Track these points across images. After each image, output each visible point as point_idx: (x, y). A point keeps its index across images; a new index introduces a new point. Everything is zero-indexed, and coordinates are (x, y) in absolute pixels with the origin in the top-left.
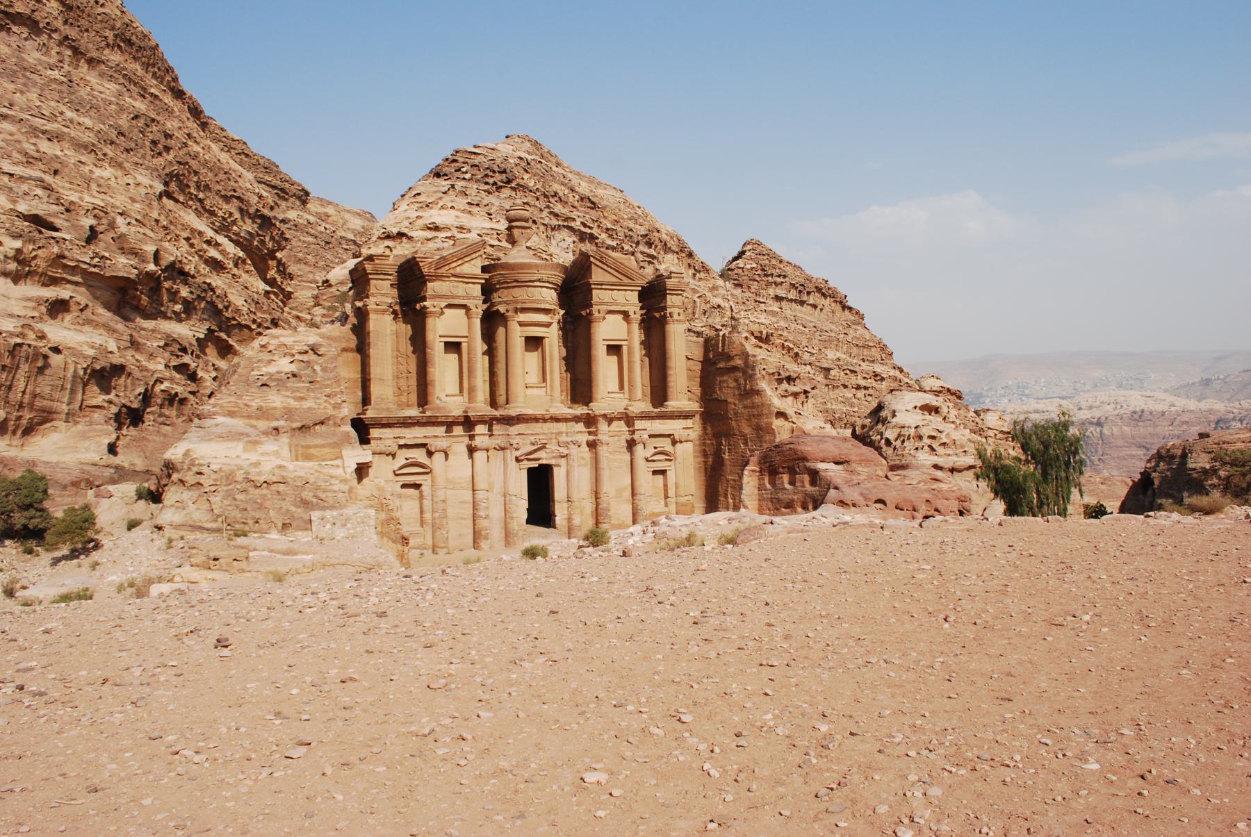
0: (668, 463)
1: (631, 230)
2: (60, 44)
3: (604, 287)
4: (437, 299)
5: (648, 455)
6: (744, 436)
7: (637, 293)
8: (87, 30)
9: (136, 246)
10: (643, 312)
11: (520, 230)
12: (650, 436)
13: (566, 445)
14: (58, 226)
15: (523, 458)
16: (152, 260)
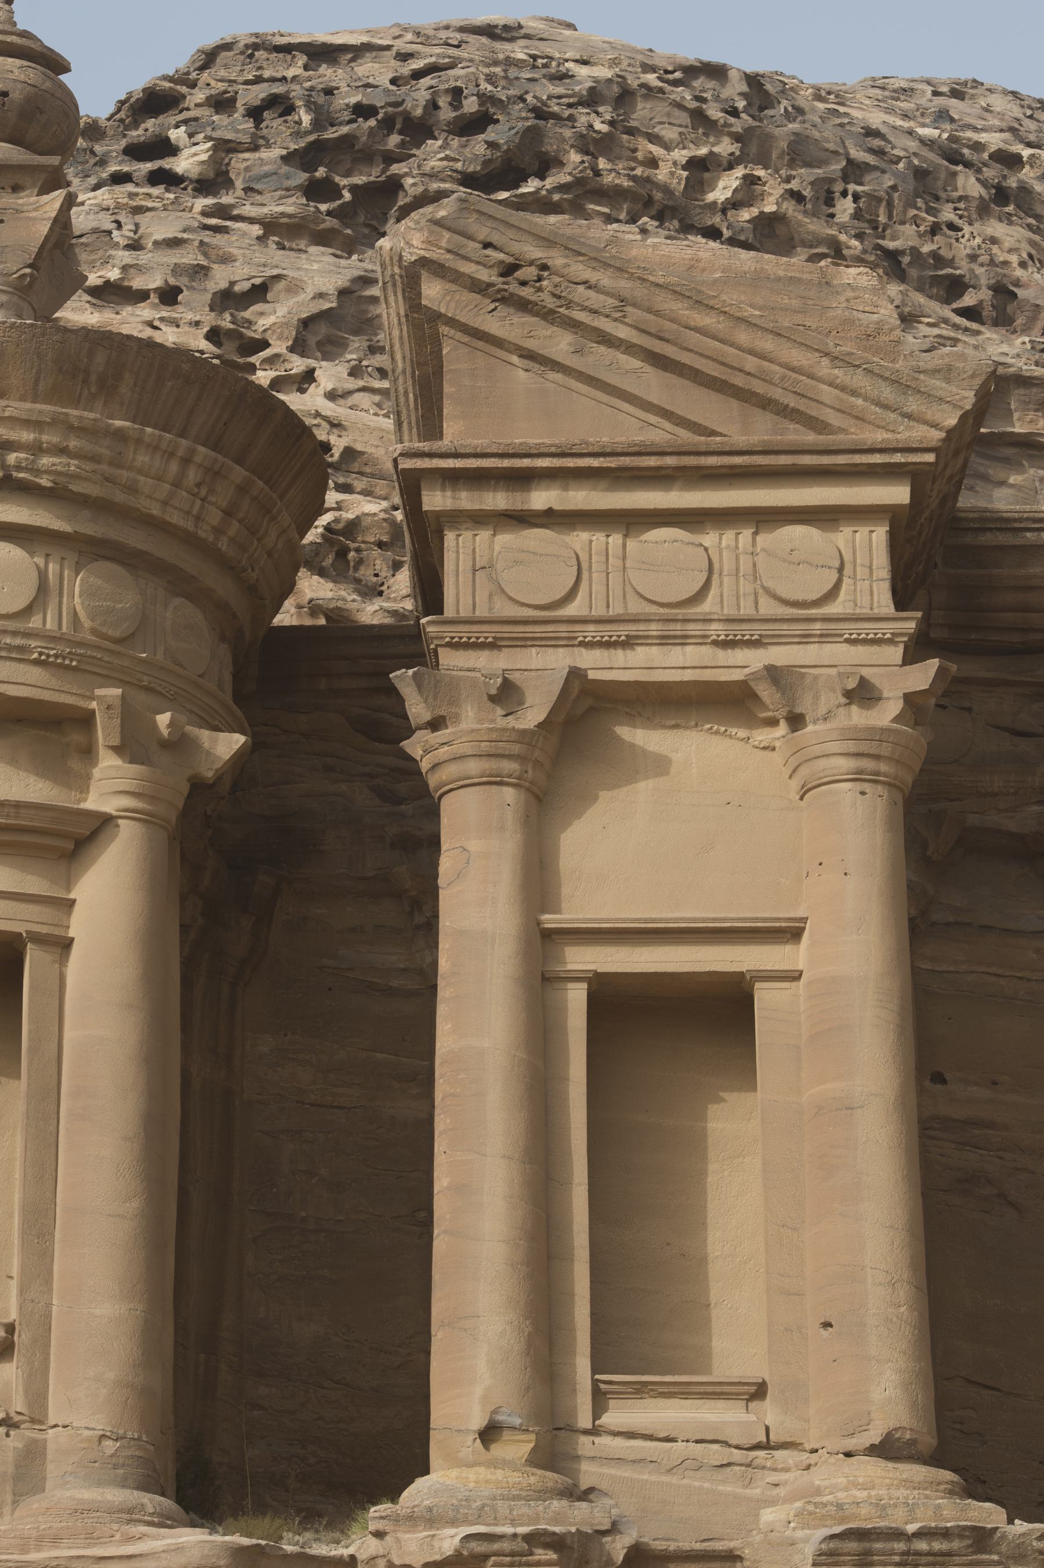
3: (541, 499)
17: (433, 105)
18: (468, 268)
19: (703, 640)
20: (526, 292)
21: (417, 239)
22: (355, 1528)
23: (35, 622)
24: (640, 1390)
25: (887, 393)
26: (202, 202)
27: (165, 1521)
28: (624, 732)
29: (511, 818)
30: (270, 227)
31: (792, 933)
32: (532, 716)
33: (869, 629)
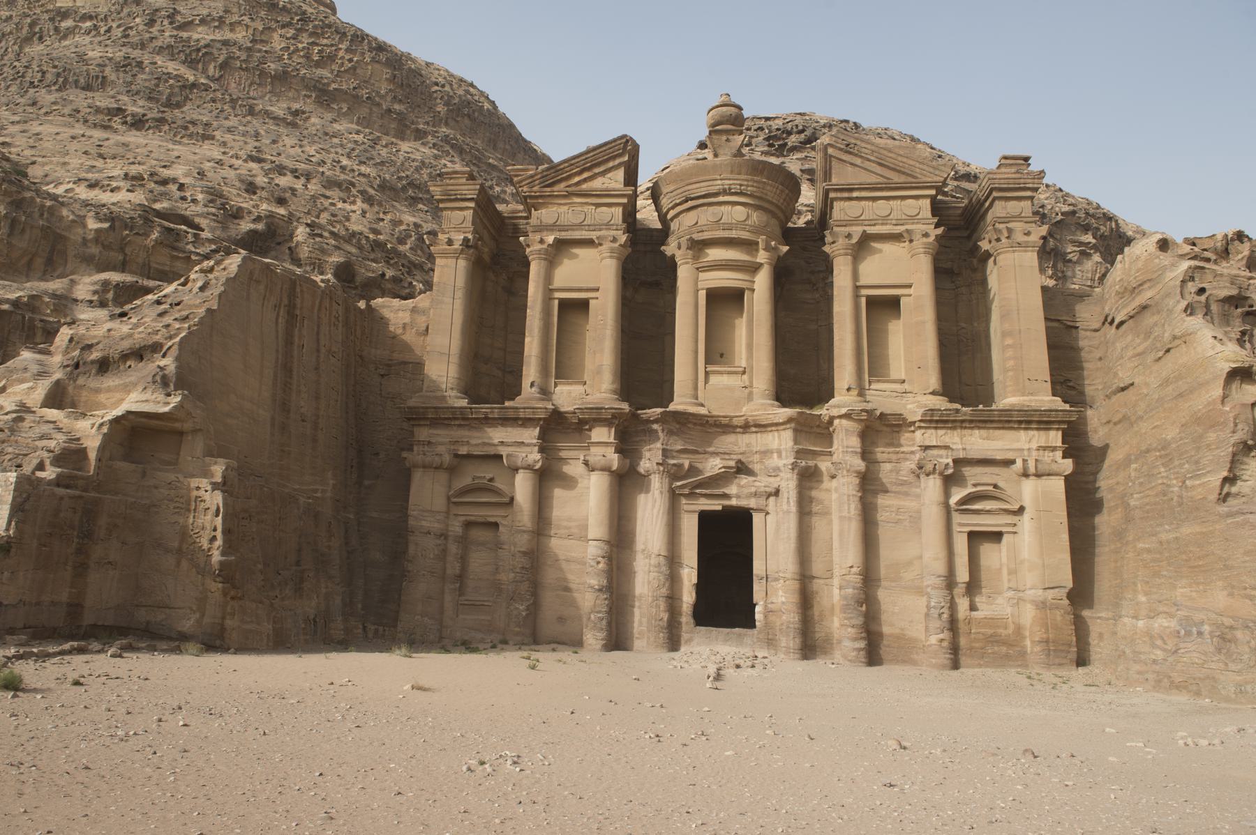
0: (1010, 519)
1: (1043, 207)
2: (382, 116)
3: (855, 194)
4: (545, 233)
5: (954, 500)
6: (1165, 446)
7: (928, 201)
8: (419, 106)
9: (313, 255)
10: (940, 231)
11: (724, 138)
12: (957, 462)
13: (775, 472)
14: (203, 226)
15: (686, 491)
16: (332, 271)
17: (792, 128)
18: (838, 145)
19: (891, 224)
20: (851, 150)
21: (827, 139)
22: (821, 408)
23: (747, 223)
24: (878, 381)
25: (932, 170)
26: (748, 148)
27: (779, 407)
28: (872, 244)
29: (850, 262)
30: (762, 153)
31: (910, 286)
32: (854, 241)
33: (927, 221)
